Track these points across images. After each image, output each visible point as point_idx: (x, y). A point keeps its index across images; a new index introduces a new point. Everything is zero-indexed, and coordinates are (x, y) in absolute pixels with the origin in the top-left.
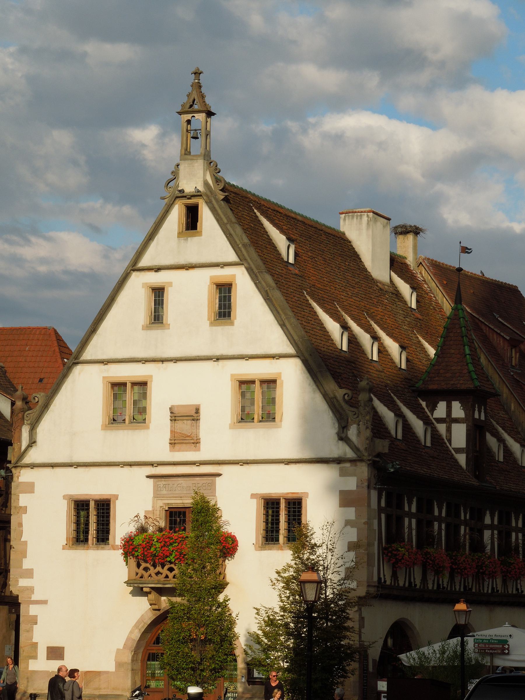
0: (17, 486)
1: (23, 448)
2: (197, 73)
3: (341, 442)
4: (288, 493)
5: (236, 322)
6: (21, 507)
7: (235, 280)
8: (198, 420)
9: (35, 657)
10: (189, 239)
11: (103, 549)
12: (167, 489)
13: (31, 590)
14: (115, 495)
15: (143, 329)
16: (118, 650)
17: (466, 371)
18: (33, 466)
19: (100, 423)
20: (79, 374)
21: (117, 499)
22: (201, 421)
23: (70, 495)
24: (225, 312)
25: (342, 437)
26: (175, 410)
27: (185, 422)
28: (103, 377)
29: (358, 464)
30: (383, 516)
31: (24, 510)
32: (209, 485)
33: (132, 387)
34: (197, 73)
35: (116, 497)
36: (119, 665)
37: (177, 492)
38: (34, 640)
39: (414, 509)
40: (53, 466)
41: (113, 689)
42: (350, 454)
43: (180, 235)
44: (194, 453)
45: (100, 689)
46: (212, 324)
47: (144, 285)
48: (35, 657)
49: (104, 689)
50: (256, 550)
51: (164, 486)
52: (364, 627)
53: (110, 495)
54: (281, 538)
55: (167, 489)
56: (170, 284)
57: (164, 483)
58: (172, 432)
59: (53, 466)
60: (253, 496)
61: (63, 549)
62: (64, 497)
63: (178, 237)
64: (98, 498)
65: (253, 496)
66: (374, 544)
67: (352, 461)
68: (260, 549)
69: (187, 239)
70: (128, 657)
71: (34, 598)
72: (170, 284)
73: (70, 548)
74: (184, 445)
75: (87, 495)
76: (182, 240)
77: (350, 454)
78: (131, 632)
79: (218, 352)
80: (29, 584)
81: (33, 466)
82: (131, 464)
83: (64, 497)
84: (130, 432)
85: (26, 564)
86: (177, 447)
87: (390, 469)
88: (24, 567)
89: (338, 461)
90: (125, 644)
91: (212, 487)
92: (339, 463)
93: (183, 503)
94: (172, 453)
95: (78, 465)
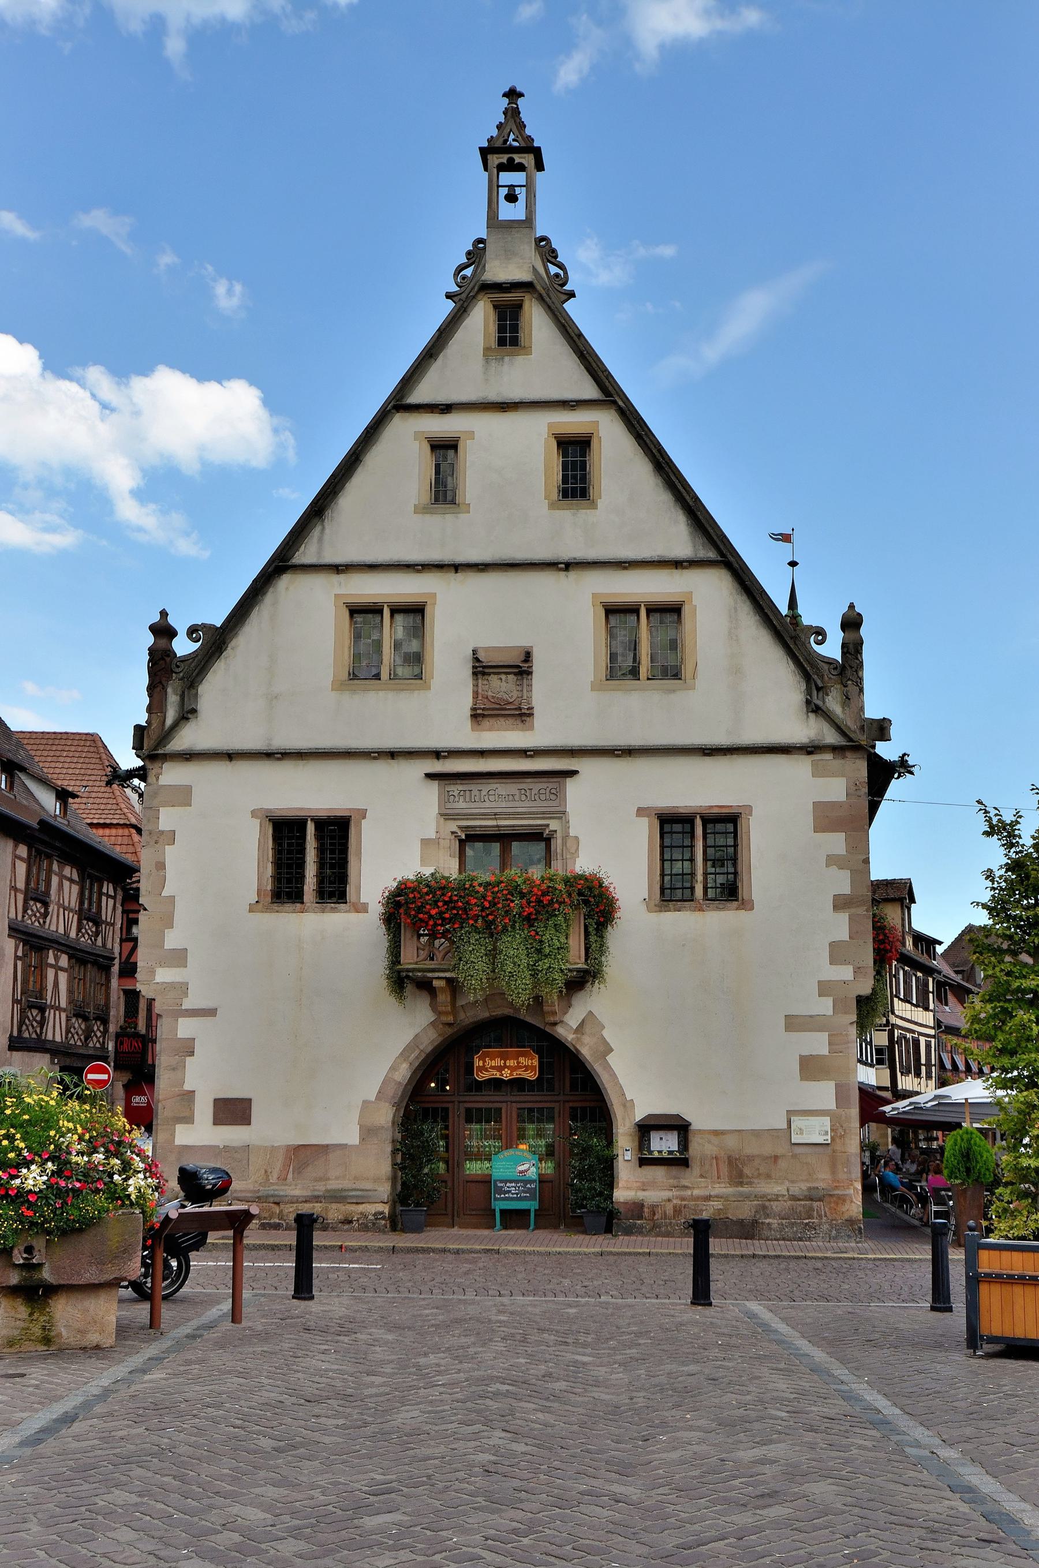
1: (169, 722)
2: (513, 94)
3: (812, 716)
5: (601, 503)
6: (162, 832)
8: (530, 673)
9: (189, 1120)
10: (507, 359)
12: (467, 800)
13: (182, 989)
16: (365, 1102)
18: (189, 756)
20: (287, 589)
21: (364, 817)
26: (481, 656)
27: (503, 677)
29: (848, 754)
31: (171, 837)
32: (553, 791)
33: (392, 616)
34: (513, 94)
36: (367, 1132)
37: (487, 804)
38: (187, 1087)
40: (230, 756)
41: (356, 1178)
42: (831, 737)
44: (521, 733)
45: (329, 1179)
46: (552, 506)
47: (417, 435)
48: (189, 1120)
50: (649, 910)
51: (462, 793)
53: (350, 809)
55: (467, 800)
57: (461, 788)
58: (476, 694)
59: (230, 756)
60: (641, 812)
61: (250, 911)
62: (254, 814)
64: (323, 814)
65: (641, 812)
67: (834, 749)
68: (658, 909)
69: (503, 359)
70: (385, 1116)
72: (471, 434)
73: (266, 910)
74: (502, 720)
77: (831, 737)
78: (393, 1068)
79: (567, 554)
81: (189, 756)
82: (392, 754)
83: (254, 814)
84: (391, 695)
86: (486, 723)
89: (810, 749)
90: (379, 1092)
91: (559, 795)
92: (809, 753)
93: (497, 826)
95: (285, 755)
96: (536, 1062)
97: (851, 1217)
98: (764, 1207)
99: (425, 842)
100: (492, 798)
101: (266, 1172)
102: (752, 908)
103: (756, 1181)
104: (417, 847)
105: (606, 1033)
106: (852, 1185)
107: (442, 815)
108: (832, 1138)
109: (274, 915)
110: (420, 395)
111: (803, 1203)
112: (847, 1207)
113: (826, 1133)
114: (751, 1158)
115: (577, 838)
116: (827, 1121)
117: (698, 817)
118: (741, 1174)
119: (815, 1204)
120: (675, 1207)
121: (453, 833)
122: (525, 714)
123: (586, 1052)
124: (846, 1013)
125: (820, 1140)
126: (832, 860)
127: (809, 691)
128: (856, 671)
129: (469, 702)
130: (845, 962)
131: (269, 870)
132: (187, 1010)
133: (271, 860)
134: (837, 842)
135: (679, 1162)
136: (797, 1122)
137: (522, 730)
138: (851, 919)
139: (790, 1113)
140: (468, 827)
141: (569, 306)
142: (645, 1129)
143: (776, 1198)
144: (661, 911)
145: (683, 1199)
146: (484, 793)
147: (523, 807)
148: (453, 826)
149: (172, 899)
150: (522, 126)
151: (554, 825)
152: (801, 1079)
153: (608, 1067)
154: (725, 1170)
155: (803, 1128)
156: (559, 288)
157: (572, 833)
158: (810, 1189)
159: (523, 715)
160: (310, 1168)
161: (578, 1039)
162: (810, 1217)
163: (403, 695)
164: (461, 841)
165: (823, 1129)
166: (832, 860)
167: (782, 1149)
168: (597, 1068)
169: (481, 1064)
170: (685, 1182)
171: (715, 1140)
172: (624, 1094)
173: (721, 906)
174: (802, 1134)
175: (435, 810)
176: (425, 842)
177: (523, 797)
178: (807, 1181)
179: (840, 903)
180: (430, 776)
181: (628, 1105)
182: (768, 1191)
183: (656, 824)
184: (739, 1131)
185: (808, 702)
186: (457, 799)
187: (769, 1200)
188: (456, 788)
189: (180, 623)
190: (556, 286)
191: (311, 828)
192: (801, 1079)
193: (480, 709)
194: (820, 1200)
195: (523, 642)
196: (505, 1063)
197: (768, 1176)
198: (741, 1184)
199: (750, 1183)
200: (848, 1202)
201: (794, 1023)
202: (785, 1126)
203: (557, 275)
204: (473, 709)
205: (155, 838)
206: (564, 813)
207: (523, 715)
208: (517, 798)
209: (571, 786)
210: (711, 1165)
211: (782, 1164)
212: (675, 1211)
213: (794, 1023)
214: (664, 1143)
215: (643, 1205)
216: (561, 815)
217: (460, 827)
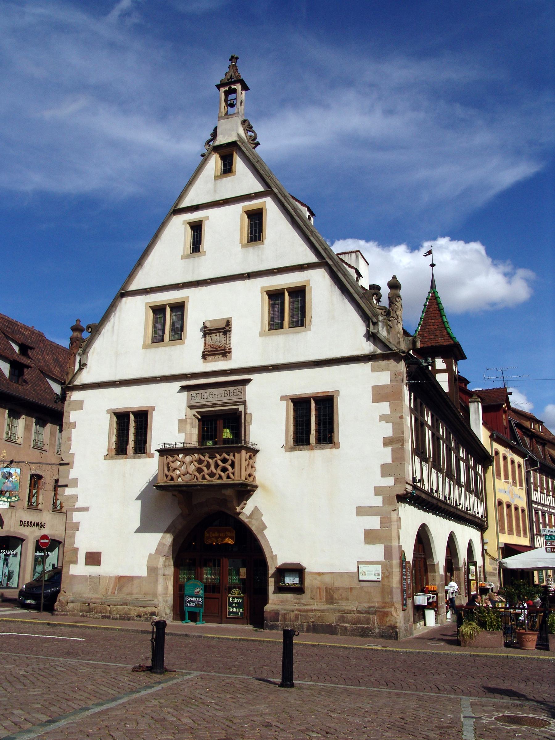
0: (69, 404)
1: (76, 371)
4: (318, 393)
7: (265, 206)
8: (230, 331)
9: (75, 562)
11: (140, 457)
12: (200, 398)
13: (75, 498)
14: (152, 406)
15: (182, 259)
16: (150, 555)
17: (445, 333)
19: (141, 343)
21: (154, 410)
22: (232, 331)
23: (113, 409)
24: (255, 236)
25: (371, 336)
26: (208, 325)
27: (218, 334)
28: (146, 303)
30: (413, 416)
31: (74, 425)
32: (240, 390)
35: (153, 408)
37: (209, 400)
38: (75, 546)
39: (430, 423)
41: (145, 594)
43: (217, 178)
44: (226, 362)
45: (132, 594)
46: (243, 246)
48: (75, 562)
49: (136, 594)
50: (286, 451)
52: (401, 529)
54: (313, 438)
55: (200, 398)
56: (207, 218)
58: (205, 343)
60: (283, 398)
61: (105, 459)
62: (108, 412)
63: (215, 180)
65: (283, 398)
66: (408, 441)
68: (290, 450)
71: (78, 505)
72: (207, 218)
73: (111, 458)
75: (127, 408)
76: (219, 181)
80: (74, 493)
83: (108, 412)
85: (73, 474)
86: (209, 358)
87: (423, 364)
88: (70, 478)
90: (156, 550)
91: (243, 393)
94: (205, 364)
96: (234, 535)
97: (391, 624)
98: (343, 617)
99: (181, 421)
100: (211, 396)
101: (106, 589)
102: (339, 447)
103: (340, 602)
104: (177, 423)
105: (263, 518)
106: (393, 605)
107: (189, 407)
108: (383, 578)
109: (115, 461)
111: (364, 615)
112: (388, 619)
113: (379, 575)
114: (338, 589)
115: (251, 414)
116: (379, 568)
117: (312, 399)
118: (332, 598)
119: (371, 616)
120: (296, 615)
121: (194, 415)
122: (227, 352)
123: (254, 529)
124: (390, 505)
125: (375, 578)
126: (383, 418)
127: (368, 326)
128: (395, 312)
129: (202, 349)
130: (390, 476)
131: (114, 439)
132: (77, 508)
133: (115, 433)
134: (385, 408)
135: (299, 590)
136: (363, 568)
137: (226, 360)
138: (392, 450)
139: (359, 563)
140: (201, 412)
142: (283, 571)
143: (350, 612)
144: (292, 451)
145: (300, 611)
146: (207, 394)
147: (226, 399)
148: (194, 412)
149: (73, 454)
151: (241, 408)
152: (365, 544)
153: (264, 537)
154: (324, 595)
155: (366, 571)
156: (252, 142)
157: (249, 411)
158: (370, 607)
159: (225, 353)
160: (125, 588)
161: (250, 522)
162: (369, 624)
163: (173, 347)
164: (199, 420)
165: (377, 572)
166: (383, 418)
167: (355, 584)
168: (259, 537)
169: (208, 535)
170: (303, 601)
171: (318, 578)
172: (272, 552)
173: (322, 447)
174: (365, 575)
175: (185, 404)
176: (181, 421)
177: (226, 395)
178: (368, 602)
179: (387, 442)
180: (184, 388)
181: (274, 557)
182: (346, 608)
183: (291, 405)
184: (332, 573)
185: (368, 331)
186: (195, 398)
187: (345, 613)
188: (194, 393)
189: (84, 325)
190: (250, 141)
191: (132, 417)
192: (365, 544)
193: (206, 351)
194: (373, 614)
195: (227, 316)
196: (219, 535)
197: (347, 599)
198: (332, 603)
199: (337, 603)
200: (390, 615)
201: (362, 511)
202: (356, 570)
204: (203, 352)
205: (68, 426)
206: (245, 402)
207: (225, 353)
208: (223, 395)
209: (249, 388)
210: (316, 592)
211: (355, 592)
212: (295, 617)
213: (362, 511)
214: (291, 580)
215: (279, 614)
216: (244, 403)
217: (198, 412)
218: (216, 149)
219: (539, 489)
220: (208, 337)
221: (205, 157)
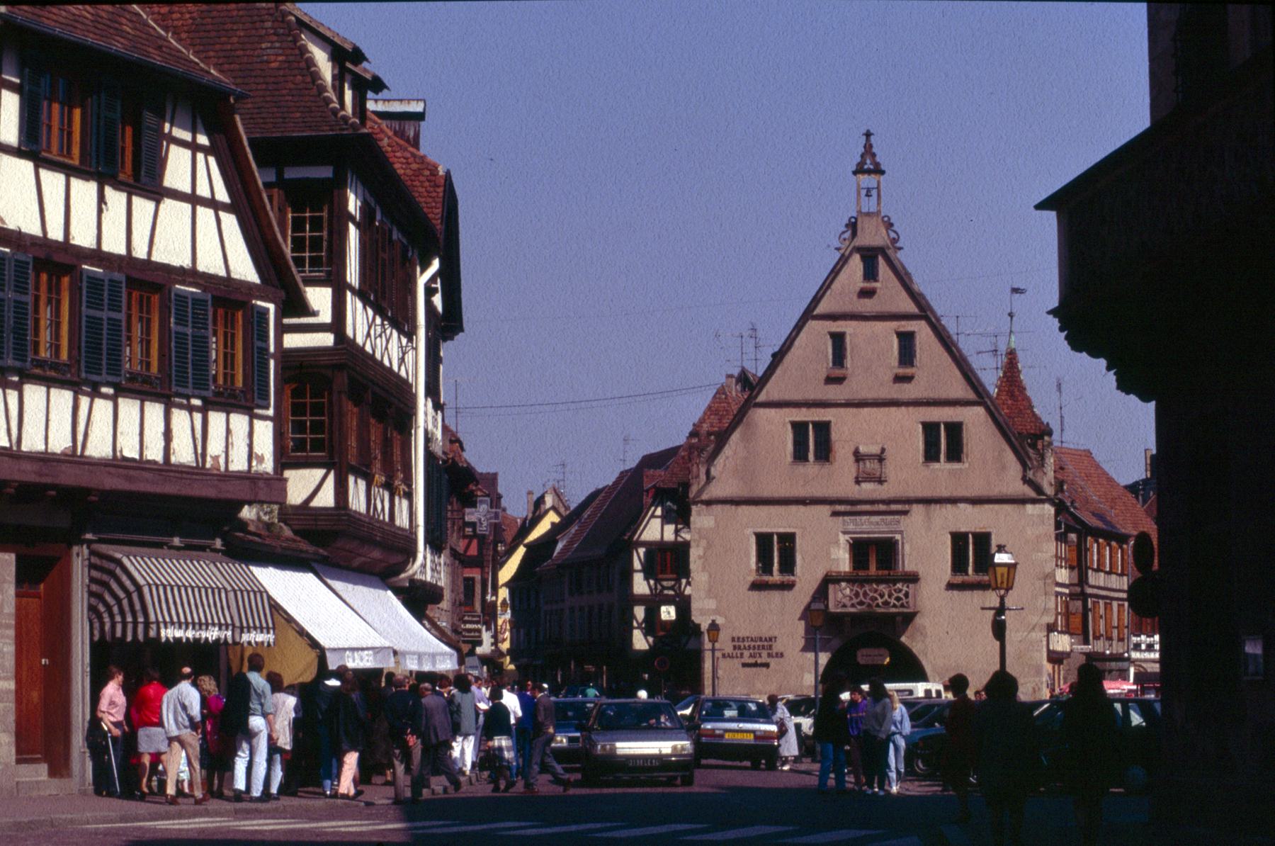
2: (868, 135)
34: (868, 135)
110: (821, 308)
121: (847, 541)
141: (900, 255)
148: (847, 537)
150: (874, 155)
151: (898, 537)
164: (850, 545)
203: (894, 239)
217: (851, 538)
218: (858, 250)
219: (1115, 632)
220: (861, 463)
221: (843, 260)
